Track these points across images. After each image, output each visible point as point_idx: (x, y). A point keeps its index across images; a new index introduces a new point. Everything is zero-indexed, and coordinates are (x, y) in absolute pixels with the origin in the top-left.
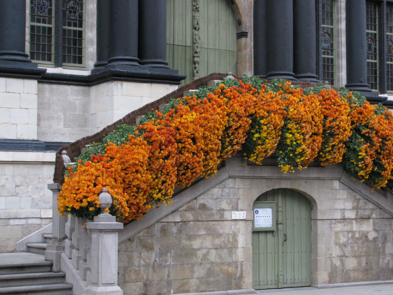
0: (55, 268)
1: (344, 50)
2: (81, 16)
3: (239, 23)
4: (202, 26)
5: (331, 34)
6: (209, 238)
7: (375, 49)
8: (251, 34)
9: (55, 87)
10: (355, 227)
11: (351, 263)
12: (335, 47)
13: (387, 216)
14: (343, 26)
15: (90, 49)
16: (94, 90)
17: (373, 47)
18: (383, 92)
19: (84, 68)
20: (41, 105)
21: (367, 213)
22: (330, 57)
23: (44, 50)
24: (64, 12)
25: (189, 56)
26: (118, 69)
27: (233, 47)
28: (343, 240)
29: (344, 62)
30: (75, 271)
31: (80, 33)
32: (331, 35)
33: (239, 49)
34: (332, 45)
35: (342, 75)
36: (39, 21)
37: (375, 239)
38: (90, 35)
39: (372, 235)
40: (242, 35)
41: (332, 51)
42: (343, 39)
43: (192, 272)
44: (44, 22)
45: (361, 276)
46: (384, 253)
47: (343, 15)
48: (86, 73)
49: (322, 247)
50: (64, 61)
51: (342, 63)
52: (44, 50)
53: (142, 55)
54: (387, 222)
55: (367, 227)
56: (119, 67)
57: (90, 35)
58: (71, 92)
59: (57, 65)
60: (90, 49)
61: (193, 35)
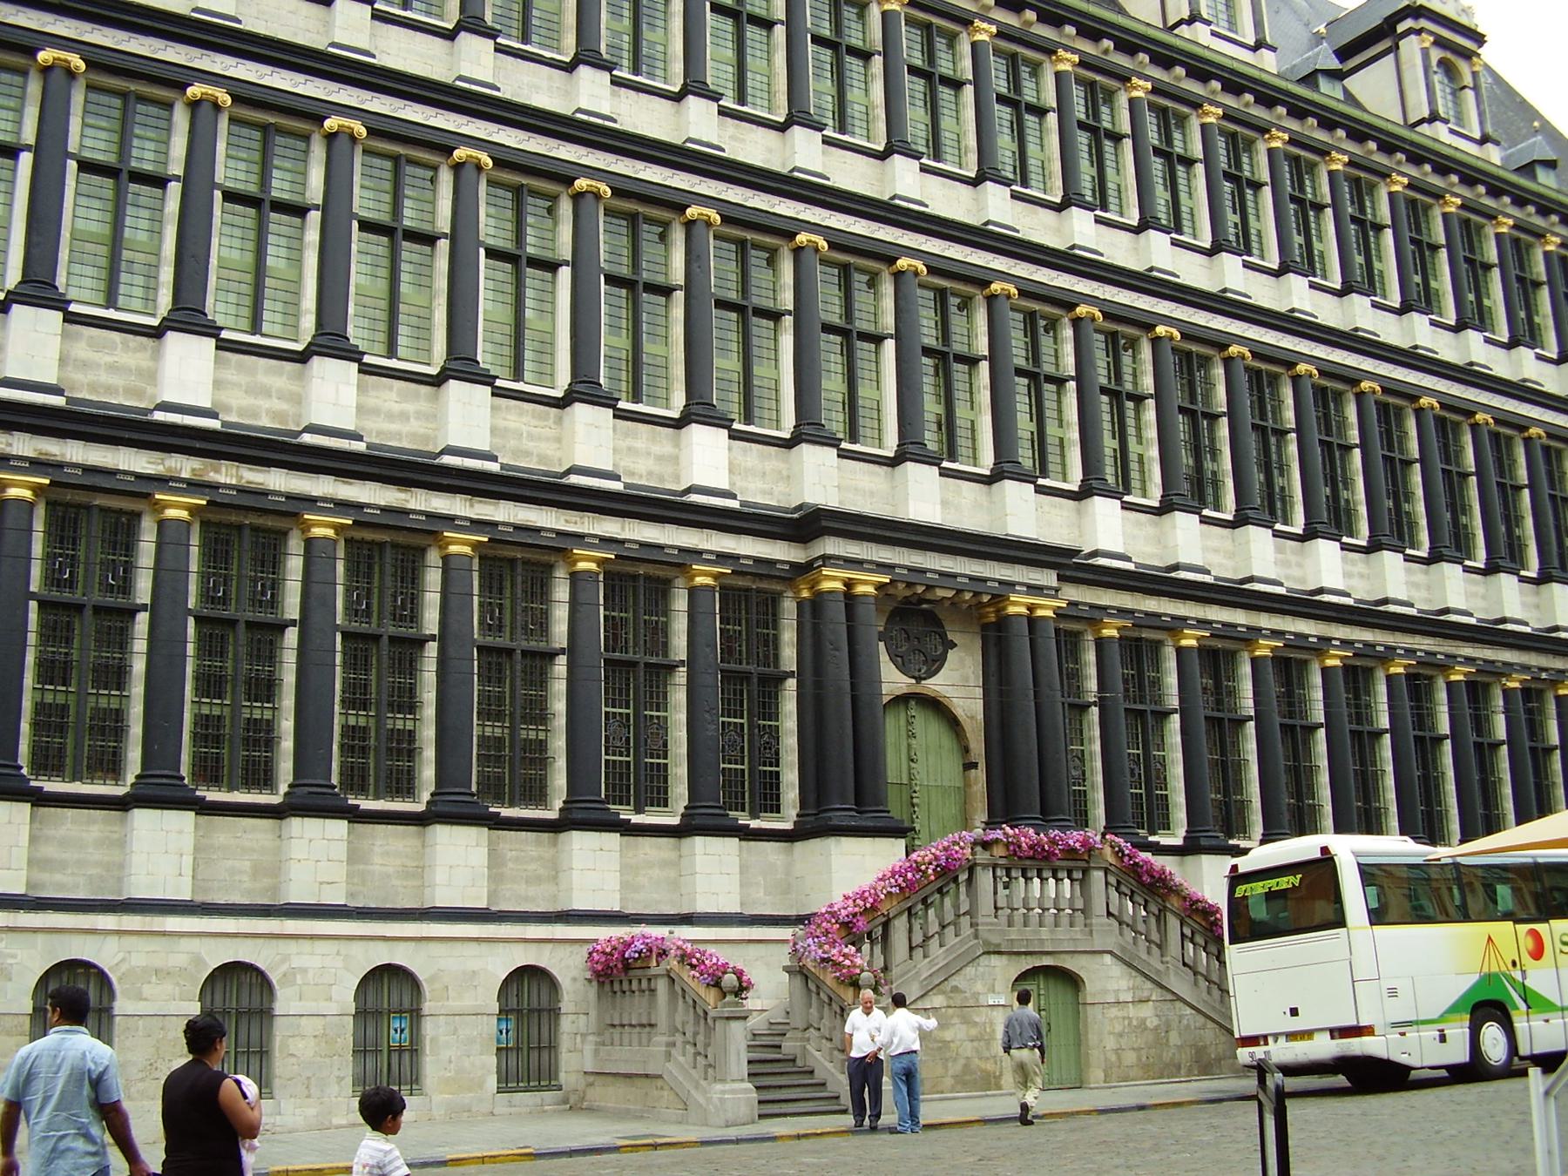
0: (799, 1062)
1: (1099, 779)
2: (777, 753)
3: (966, 750)
4: (920, 756)
5: (1081, 757)
6: (964, 1027)
10: (1132, 1011)
11: (1130, 1058)
12: (1088, 774)
13: (1170, 997)
14: (1097, 747)
15: (790, 794)
16: (800, 847)
18: (1153, 833)
19: (782, 820)
20: (743, 869)
21: (1146, 994)
25: (905, 797)
26: (835, 822)
27: (959, 783)
28: (1118, 1028)
29: (1100, 796)
30: (828, 1065)
31: (778, 773)
32: (1082, 760)
33: (967, 784)
35: (1099, 813)
37: (1156, 1028)
38: (790, 777)
39: (1152, 1022)
40: (970, 766)
42: (1099, 764)
43: (946, 1068)
45: (1141, 1073)
46: (1167, 1044)
47: (1097, 733)
48: (788, 826)
49: (1093, 1038)
51: (1098, 797)
53: (859, 800)
54: (1169, 1005)
55: (1147, 1011)
56: (837, 818)
57: (790, 777)
58: (770, 851)
59: (754, 816)
60: (790, 794)
61: (910, 768)
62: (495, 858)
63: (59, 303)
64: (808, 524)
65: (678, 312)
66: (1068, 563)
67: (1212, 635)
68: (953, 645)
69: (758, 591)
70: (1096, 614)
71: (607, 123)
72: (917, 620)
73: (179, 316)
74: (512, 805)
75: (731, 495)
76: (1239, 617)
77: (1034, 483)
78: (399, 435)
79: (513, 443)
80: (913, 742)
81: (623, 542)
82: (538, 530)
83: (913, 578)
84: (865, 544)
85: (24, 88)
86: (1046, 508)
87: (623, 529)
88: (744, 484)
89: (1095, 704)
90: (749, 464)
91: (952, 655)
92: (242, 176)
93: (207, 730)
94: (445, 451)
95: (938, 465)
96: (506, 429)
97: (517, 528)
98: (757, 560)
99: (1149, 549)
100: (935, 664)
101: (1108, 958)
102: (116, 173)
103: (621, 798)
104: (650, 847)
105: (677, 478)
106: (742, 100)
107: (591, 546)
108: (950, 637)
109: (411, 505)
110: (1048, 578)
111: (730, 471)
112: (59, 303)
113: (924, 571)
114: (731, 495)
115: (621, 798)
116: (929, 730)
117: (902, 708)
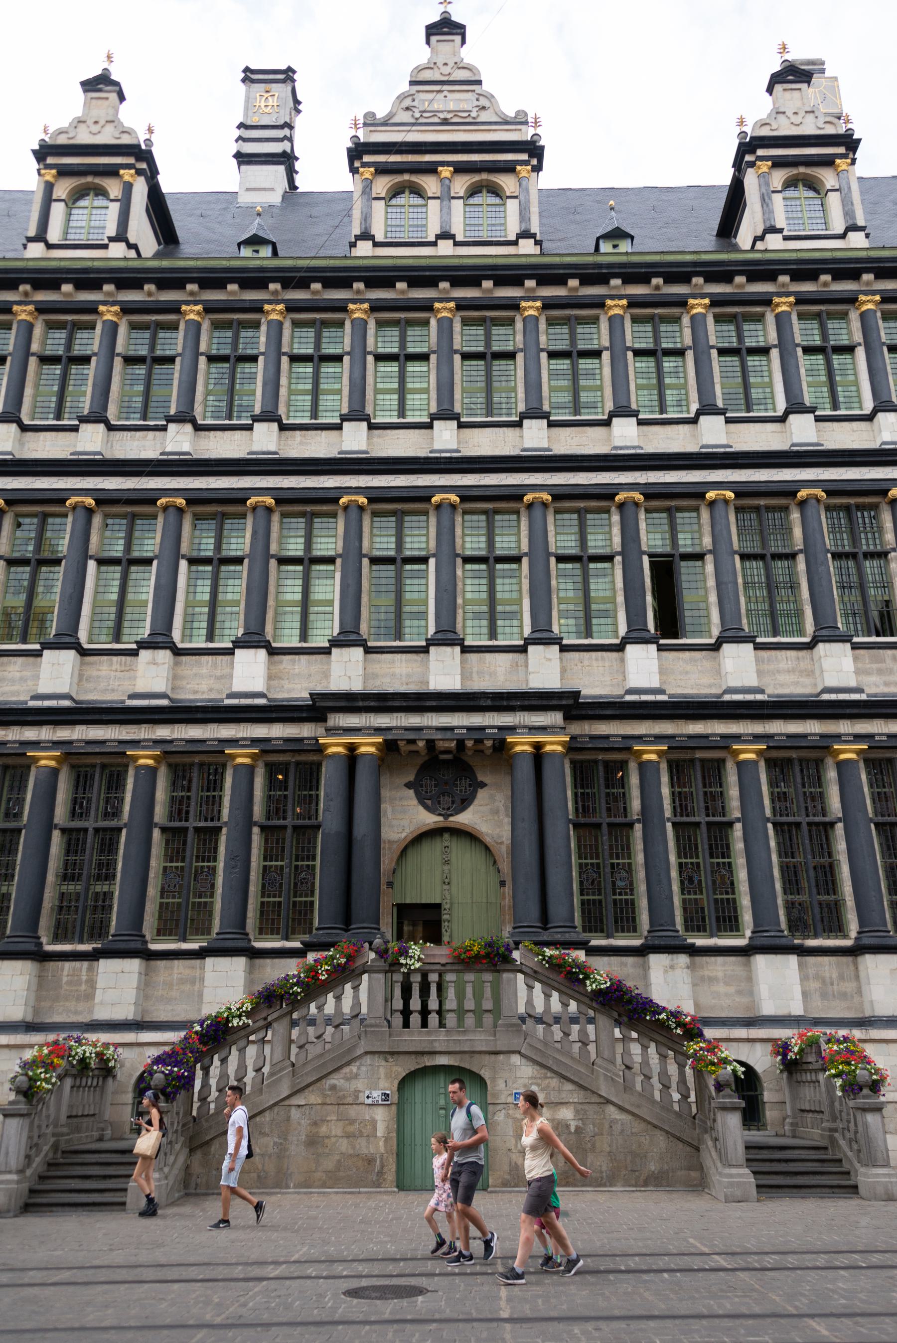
7: (700, 881)
8: (509, 883)
9: (277, 961)
14: (640, 858)
17: (696, 879)
22: (629, 897)
23: (273, 924)
24: (296, 884)
34: (631, 883)
36: (269, 896)
40: (503, 883)
41: (632, 890)
44: (275, 896)
50: (293, 933)
52: (273, 924)
62: (41, 985)
63: (458, 642)
64: (319, 708)
65: (710, 567)
66: (570, 705)
67: (769, 747)
68: (483, 785)
69: (298, 764)
70: (628, 743)
71: (728, 450)
72: (447, 771)
73: (537, 635)
74: (816, 936)
75: (860, 690)
76: (813, 727)
77: (657, 643)
78: (18, 693)
79: (103, 685)
80: (446, 868)
81: (171, 742)
82: (103, 742)
83: (411, 736)
84: (395, 715)
85: (427, 521)
86: (586, 663)
87: (173, 732)
88: (291, 686)
89: (638, 821)
90: (297, 671)
91: (482, 794)
92: (600, 543)
93: (64, 904)
94: (726, 692)
95: (849, 641)
96: (98, 677)
97: (88, 743)
98: (287, 740)
99: (706, 680)
100: (465, 803)
101: (516, 1059)
102: (489, 560)
103: (596, 927)
104: (718, 966)
105: (815, 685)
106: (835, 406)
107: (145, 748)
108: (481, 778)
109: (10, 738)
110: (555, 718)
111: (660, 673)
112: (458, 642)
113: (452, 729)
114: (860, 690)
115: (596, 927)
116: (463, 857)
117: (438, 840)
